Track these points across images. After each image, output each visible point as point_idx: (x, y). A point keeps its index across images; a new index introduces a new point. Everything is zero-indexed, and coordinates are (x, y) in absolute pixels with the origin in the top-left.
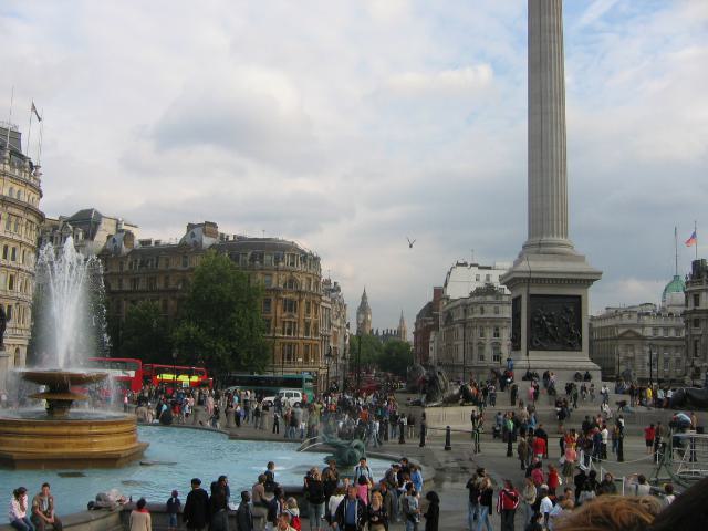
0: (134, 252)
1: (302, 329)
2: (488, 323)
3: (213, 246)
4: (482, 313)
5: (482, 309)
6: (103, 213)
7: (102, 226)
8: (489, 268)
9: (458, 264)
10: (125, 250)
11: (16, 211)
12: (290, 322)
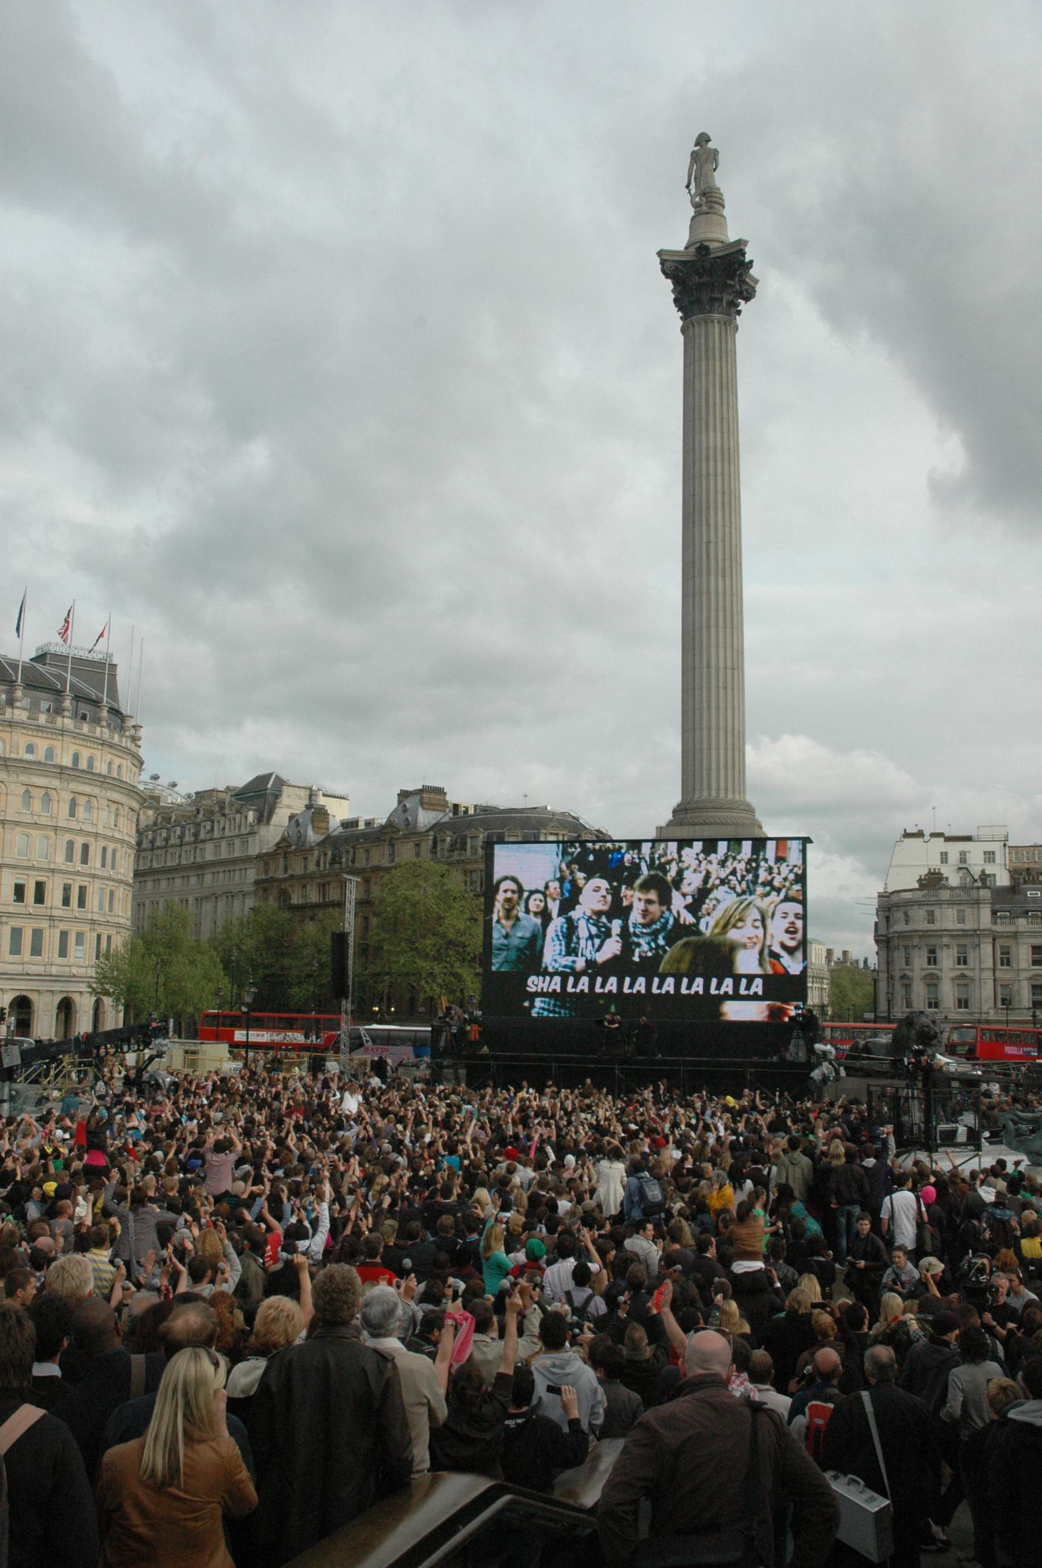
0: (330, 841)
2: (916, 941)
3: (437, 827)
4: (907, 924)
5: (906, 914)
6: (284, 776)
8: (968, 839)
9: (907, 835)
10: (313, 837)
11: (88, 789)
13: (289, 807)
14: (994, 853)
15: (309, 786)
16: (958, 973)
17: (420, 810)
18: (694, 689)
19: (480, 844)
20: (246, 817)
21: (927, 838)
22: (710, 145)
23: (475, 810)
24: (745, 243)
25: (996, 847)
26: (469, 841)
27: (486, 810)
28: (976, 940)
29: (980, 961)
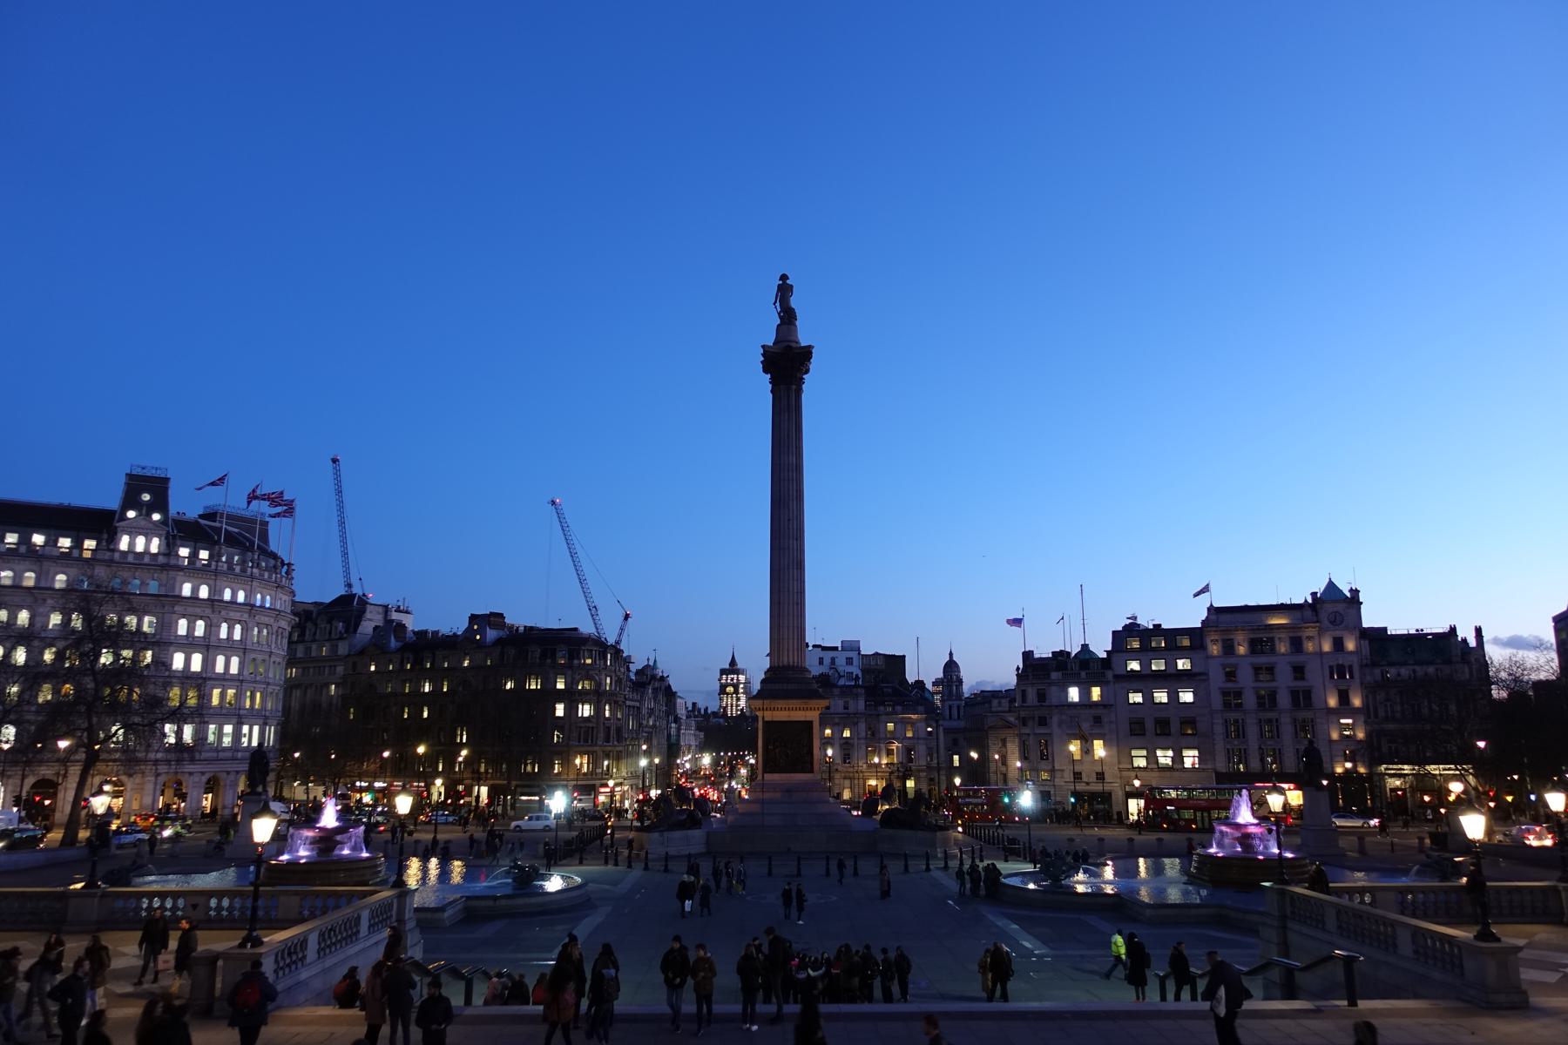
1: (602, 735)
3: (499, 642)
7: (368, 615)
8: (836, 649)
12: (589, 727)
13: (370, 620)
14: (852, 658)
15: (386, 604)
16: (844, 741)
17: (488, 629)
18: (779, 603)
19: (538, 656)
20: (336, 628)
21: (810, 648)
22: (788, 282)
23: (525, 630)
24: (813, 347)
25: (853, 654)
26: (530, 654)
27: (532, 628)
28: (856, 720)
29: (858, 734)
